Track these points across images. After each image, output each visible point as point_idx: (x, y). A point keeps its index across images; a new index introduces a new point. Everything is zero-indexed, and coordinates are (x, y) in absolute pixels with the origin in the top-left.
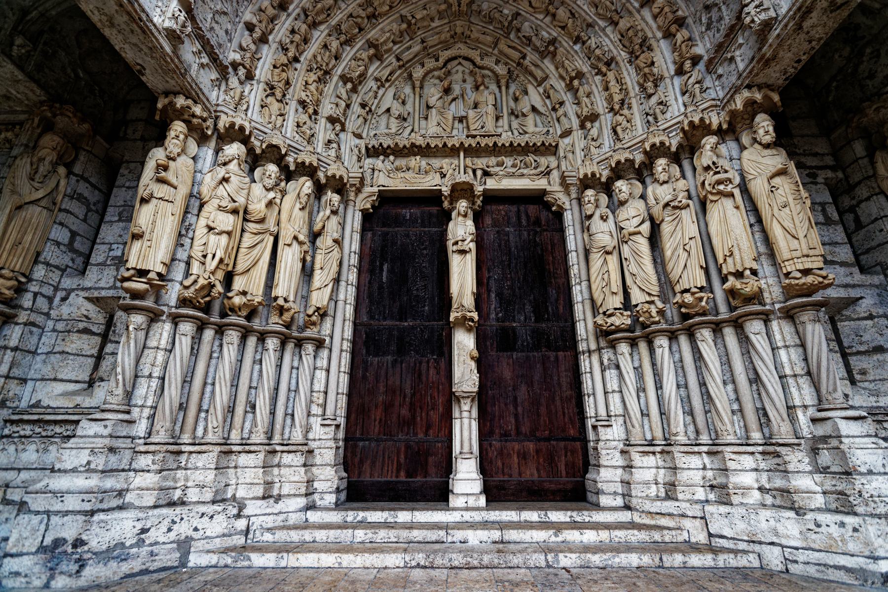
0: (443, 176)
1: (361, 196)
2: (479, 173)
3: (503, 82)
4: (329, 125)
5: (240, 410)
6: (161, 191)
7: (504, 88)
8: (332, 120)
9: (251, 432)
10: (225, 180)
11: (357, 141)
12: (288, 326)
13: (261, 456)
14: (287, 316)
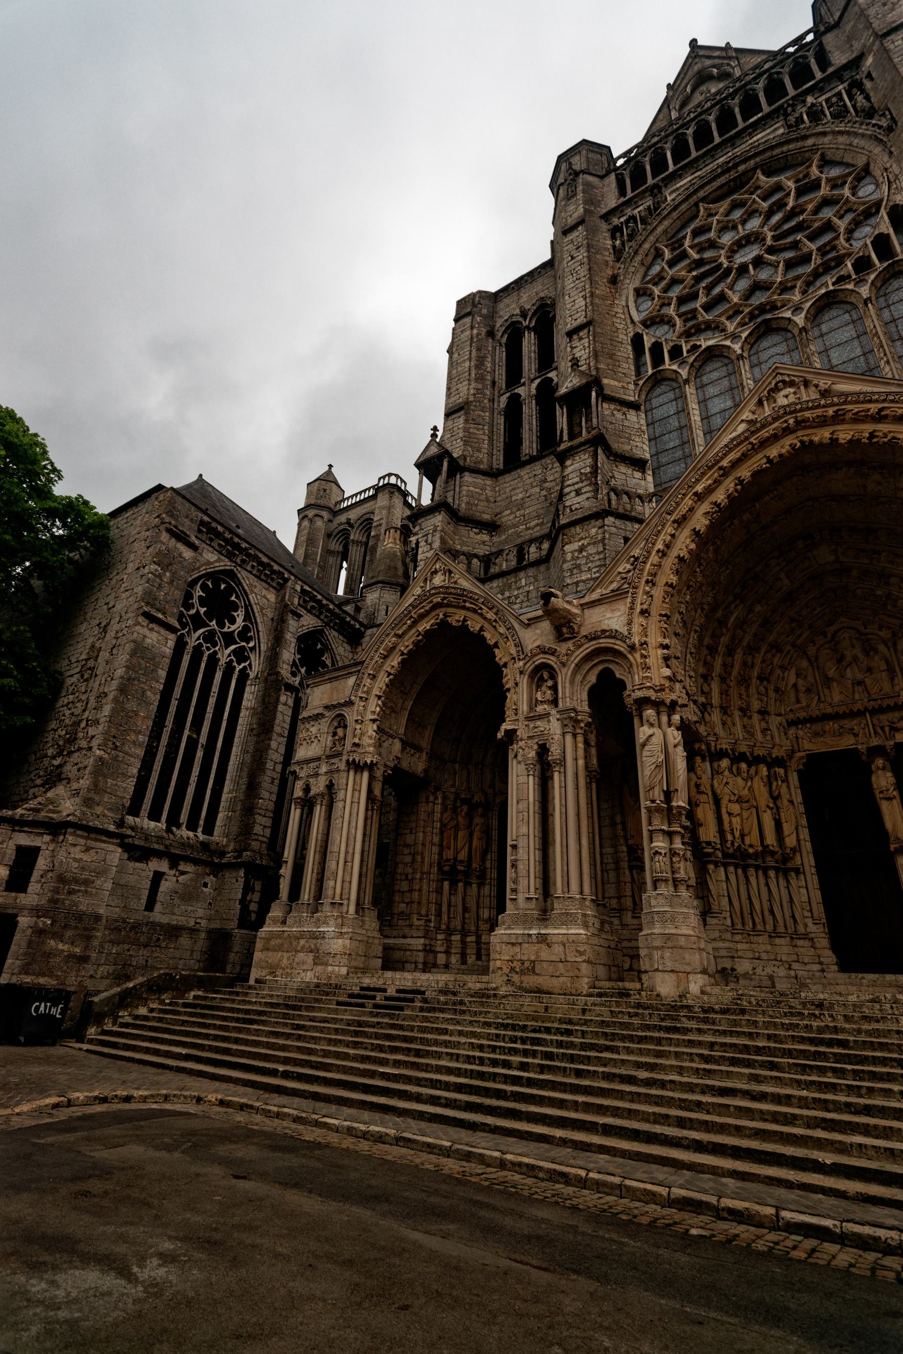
0: (856, 735)
1: (793, 761)
2: (887, 729)
3: (890, 644)
4: (759, 717)
5: (767, 913)
6: (703, 798)
7: (892, 650)
8: (759, 712)
9: (775, 926)
10: (727, 783)
11: (779, 718)
12: (776, 862)
13: (788, 939)
14: (777, 857)
